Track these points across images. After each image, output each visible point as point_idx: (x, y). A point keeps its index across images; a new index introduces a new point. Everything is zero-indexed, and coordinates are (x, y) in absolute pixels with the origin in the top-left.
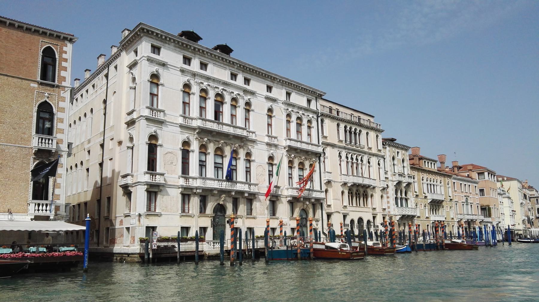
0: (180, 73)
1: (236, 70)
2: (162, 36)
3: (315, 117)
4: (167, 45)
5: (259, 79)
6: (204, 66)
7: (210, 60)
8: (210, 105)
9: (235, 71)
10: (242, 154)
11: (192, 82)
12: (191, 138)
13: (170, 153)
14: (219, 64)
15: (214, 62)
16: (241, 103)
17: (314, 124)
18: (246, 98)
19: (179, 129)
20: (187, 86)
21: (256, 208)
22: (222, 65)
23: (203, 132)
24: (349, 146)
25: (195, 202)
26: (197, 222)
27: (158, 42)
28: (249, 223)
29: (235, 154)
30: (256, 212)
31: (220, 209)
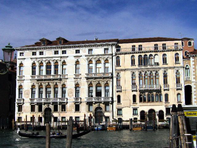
0: (30, 60)
3: (111, 57)
6: (41, 53)
8: (44, 68)
10: (60, 87)
11: (36, 62)
12: (35, 84)
16: (60, 63)
17: (110, 61)
18: (62, 60)
19: (30, 81)
20: (34, 64)
21: (67, 108)
23: (38, 80)
25: (37, 107)
26: (37, 115)
29: (56, 87)
31: (48, 110)
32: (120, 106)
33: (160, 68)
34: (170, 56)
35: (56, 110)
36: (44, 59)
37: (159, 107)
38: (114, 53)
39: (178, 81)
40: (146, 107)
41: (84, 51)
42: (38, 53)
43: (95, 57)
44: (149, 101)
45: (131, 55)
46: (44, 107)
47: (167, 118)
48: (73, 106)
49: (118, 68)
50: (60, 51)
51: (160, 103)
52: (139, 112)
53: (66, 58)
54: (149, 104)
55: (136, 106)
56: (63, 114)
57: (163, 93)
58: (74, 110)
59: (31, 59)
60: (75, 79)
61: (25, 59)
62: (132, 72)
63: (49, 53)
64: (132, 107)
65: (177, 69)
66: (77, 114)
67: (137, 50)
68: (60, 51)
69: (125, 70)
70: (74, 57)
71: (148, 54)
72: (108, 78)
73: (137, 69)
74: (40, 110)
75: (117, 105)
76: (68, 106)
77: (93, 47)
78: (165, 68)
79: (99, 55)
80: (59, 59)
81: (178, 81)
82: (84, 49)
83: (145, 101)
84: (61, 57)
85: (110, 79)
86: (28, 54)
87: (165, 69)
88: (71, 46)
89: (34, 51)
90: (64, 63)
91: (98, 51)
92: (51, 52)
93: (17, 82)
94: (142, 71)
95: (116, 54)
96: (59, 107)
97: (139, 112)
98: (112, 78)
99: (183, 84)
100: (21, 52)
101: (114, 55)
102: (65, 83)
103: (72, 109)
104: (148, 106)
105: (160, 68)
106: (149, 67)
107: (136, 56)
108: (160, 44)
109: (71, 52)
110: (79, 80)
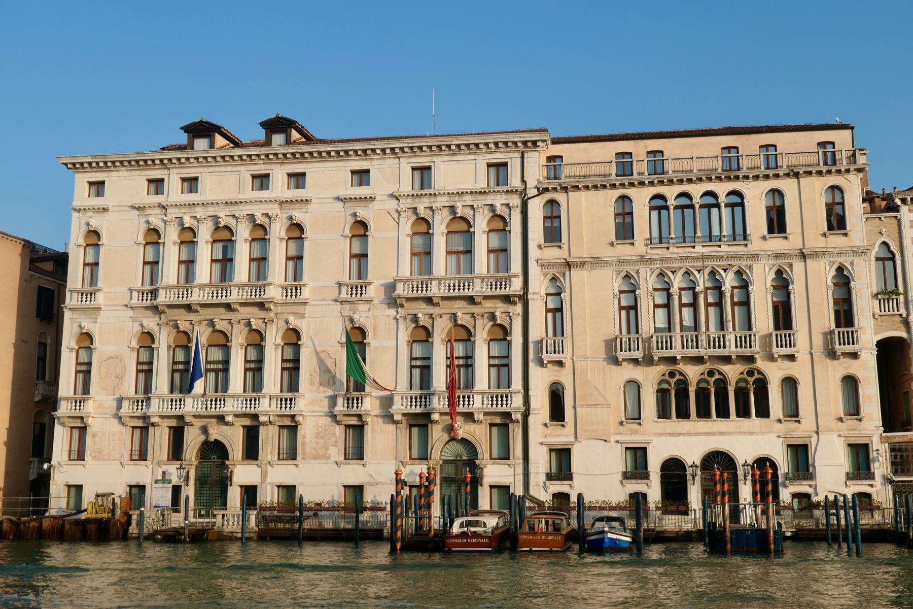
1: (262, 167)
2: (97, 163)
3: (515, 201)
4: (115, 174)
5: (328, 164)
7: (200, 170)
9: (260, 169)
13: (111, 358)
14: (223, 169)
15: (211, 169)
19: (130, 313)
21: (304, 444)
22: (229, 169)
24: (673, 250)
27: (99, 174)
28: (283, 473)
30: (304, 454)
31: (214, 451)
32: (561, 436)
33: (756, 257)
34: (806, 201)
35: (251, 452)
36: (200, 212)
37: (749, 440)
38: (531, 183)
39: (845, 315)
40: (689, 441)
41: (391, 175)
42: (173, 180)
43: (442, 201)
44: (703, 413)
45: (618, 193)
46: (193, 440)
47: (795, 495)
48: (334, 434)
49: (553, 254)
50: (279, 174)
51: (754, 422)
52: (654, 465)
53: (303, 206)
54: (703, 425)
55: (636, 439)
56: (283, 473)
57: (775, 373)
58: (336, 453)
59: (139, 209)
60: (347, 307)
61: (105, 210)
62: (618, 273)
63: (223, 184)
64: (619, 438)
65: (838, 260)
66: (354, 474)
67: (640, 167)
68: (279, 174)
69: (582, 264)
70: (343, 200)
71: (696, 191)
72: (507, 299)
73: (643, 259)
74: (176, 452)
75: (548, 431)
76: (307, 432)
77: (435, 159)
78: (777, 256)
79: (461, 194)
80: (273, 210)
81: (845, 315)
82: (391, 162)
83: (683, 414)
84: (281, 203)
85: (514, 303)
86: (127, 186)
87: (781, 262)
88: (329, 149)
89: (156, 174)
90: (297, 230)
91: (458, 174)
92: (233, 179)
93: (67, 315)
94: (667, 268)
95: (546, 190)
96: (269, 438)
97: (654, 465)
98: (524, 299)
99: (869, 331)
100: (97, 177)
101: (531, 192)
102: (301, 325)
103: (327, 449)
104: (697, 434)
105: (756, 257)
106: (699, 249)
107: (641, 198)
108: (749, 145)
109: (328, 179)
110: (363, 307)
